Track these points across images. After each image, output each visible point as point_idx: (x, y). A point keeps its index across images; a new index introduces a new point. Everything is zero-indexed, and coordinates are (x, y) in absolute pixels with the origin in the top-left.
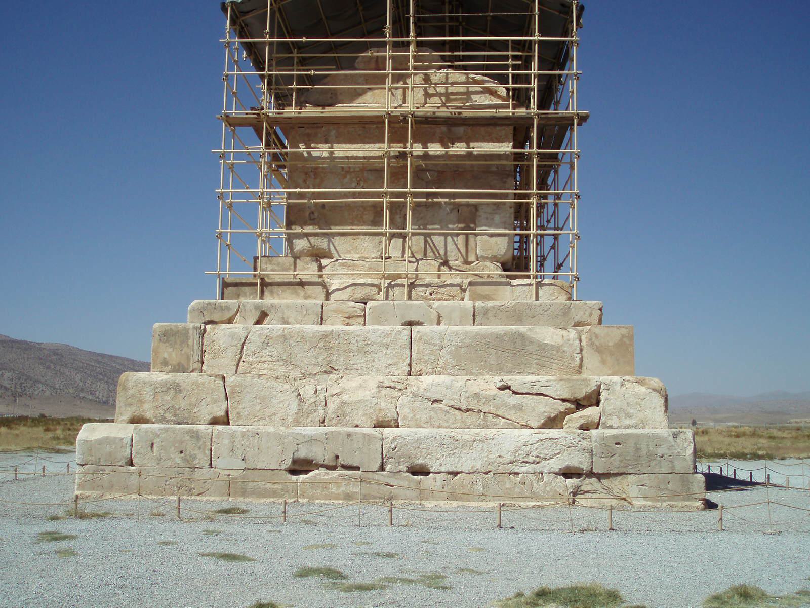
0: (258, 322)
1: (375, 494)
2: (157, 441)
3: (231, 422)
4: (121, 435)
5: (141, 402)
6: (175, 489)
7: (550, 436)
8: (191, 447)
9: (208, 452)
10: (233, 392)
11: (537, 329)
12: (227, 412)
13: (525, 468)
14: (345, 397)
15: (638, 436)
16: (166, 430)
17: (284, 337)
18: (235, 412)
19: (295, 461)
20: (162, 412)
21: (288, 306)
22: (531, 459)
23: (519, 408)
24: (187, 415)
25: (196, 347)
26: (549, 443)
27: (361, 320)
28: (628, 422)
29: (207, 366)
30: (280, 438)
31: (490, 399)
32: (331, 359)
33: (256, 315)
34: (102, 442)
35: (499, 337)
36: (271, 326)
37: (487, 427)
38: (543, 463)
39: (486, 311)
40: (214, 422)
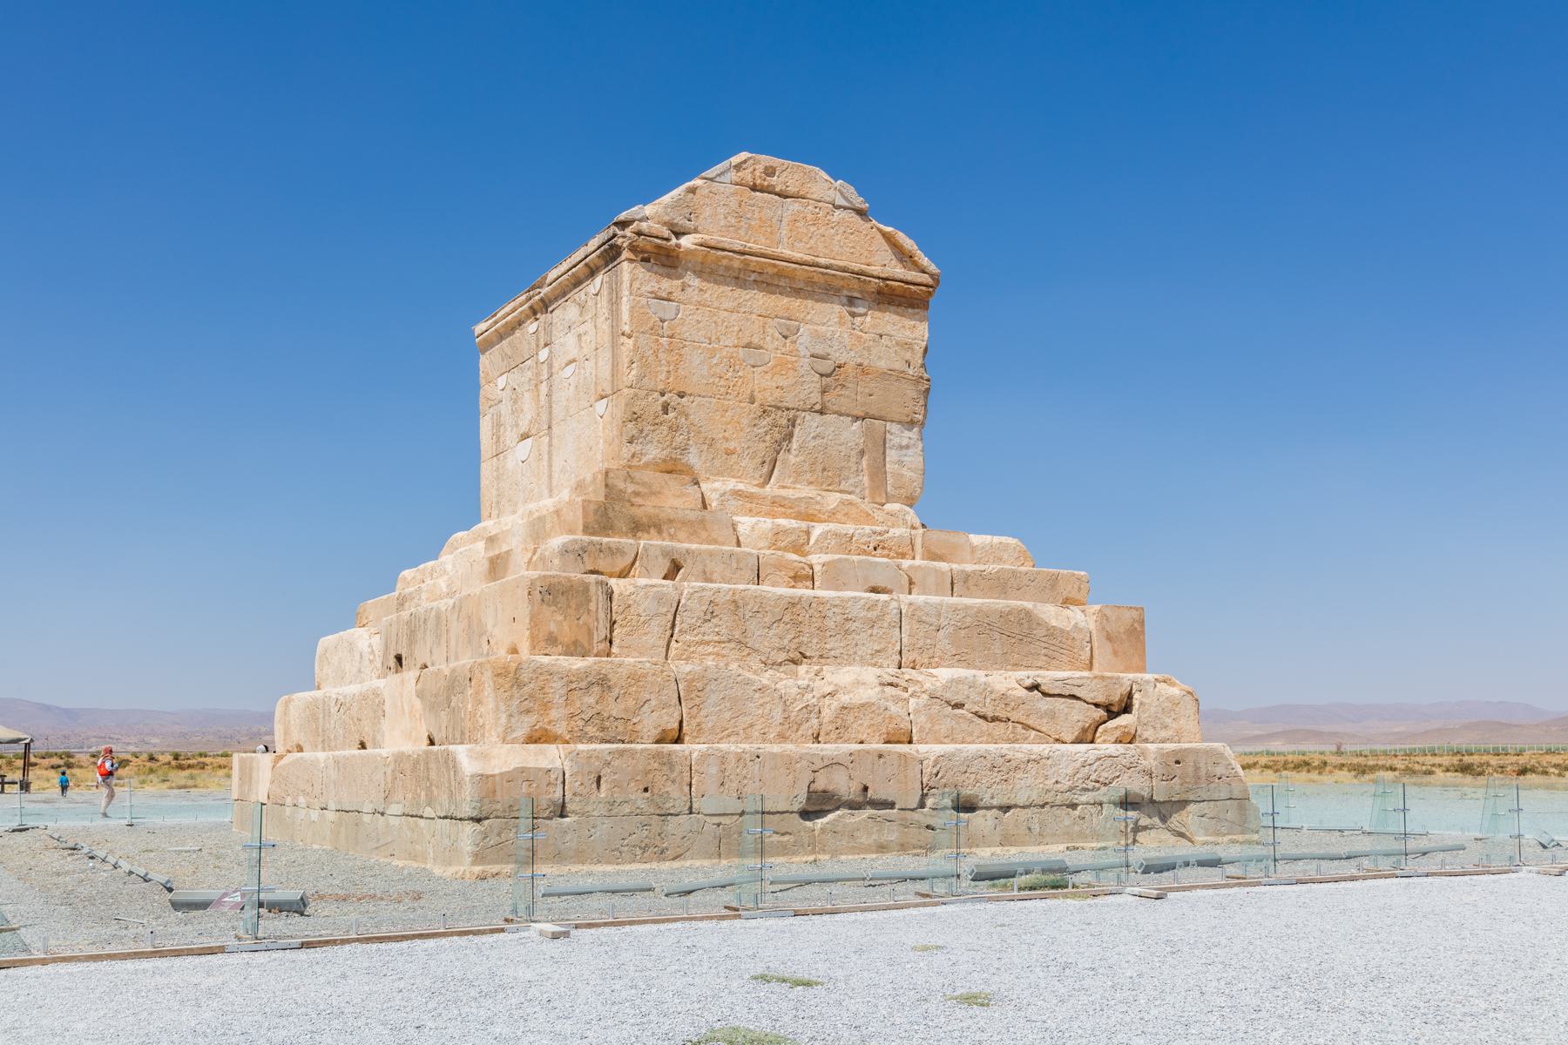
1: (914, 841)
3: (687, 738)
4: (544, 764)
5: (546, 706)
6: (639, 852)
9: (687, 789)
10: (689, 690)
12: (681, 722)
14: (845, 699)
16: (621, 753)
18: (694, 723)
20: (581, 723)
21: (711, 554)
22: (1091, 785)
23: (1052, 715)
24: (621, 729)
25: (602, 615)
26: (1108, 762)
27: (809, 583)
28: (1163, 734)
29: (621, 647)
30: (789, 762)
33: (666, 565)
35: (1002, 615)
36: (687, 585)
39: (967, 577)
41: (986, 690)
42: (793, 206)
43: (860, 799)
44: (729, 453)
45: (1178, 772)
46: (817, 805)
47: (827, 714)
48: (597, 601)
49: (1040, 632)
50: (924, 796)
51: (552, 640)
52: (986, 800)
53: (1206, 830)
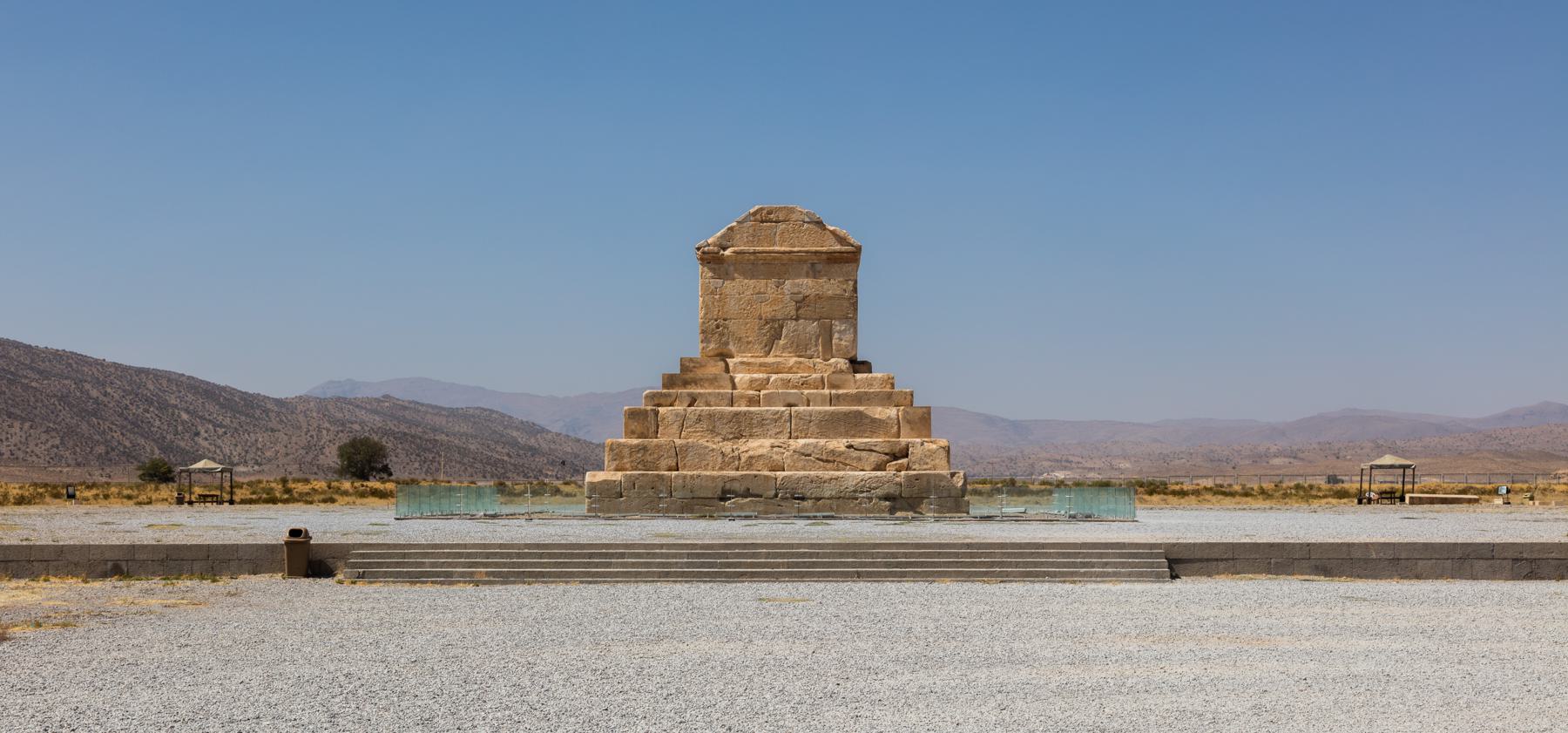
17: (711, 416)
23: (860, 459)
30: (713, 478)
31: (841, 454)
35: (846, 414)
36: (700, 408)
39: (838, 396)
40: (670, 469)
41: (823, 449)
42: (782, 226)
48: (651, 417)
51: (633, 432)
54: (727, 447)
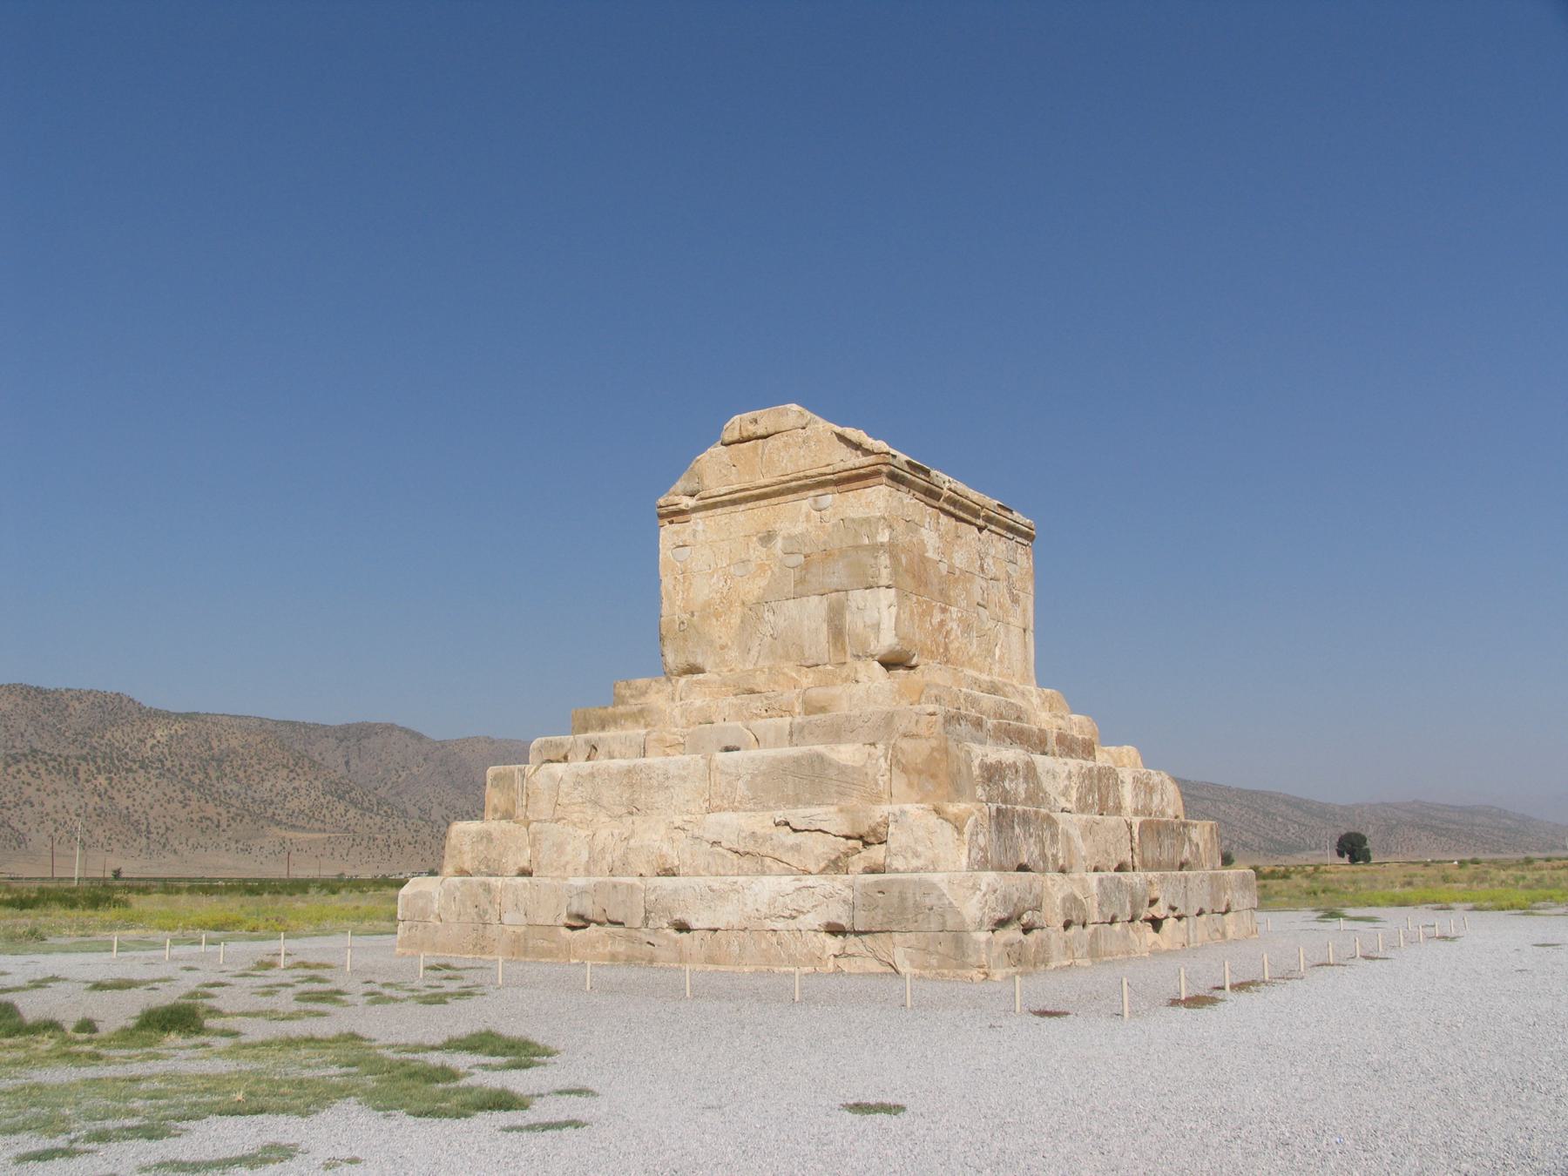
0: (589, 758)
2: (458, 894)
7: (809, 883)
8: (483, 899)
11: (842, 748)
13: (779, 925)
15: (902, 882)
17: (592, 775)
19: (570, 916)
21: (614, 738)
22: (787, 913)
23: (796, 848)
26: (805, 892)
28: (915, 863)
32: (636, 793)
34: (415, 896)
35: (797, 761)
36: (601, 762)
37: (764, 873)
38: (802, 917)
39: (802, 728)
43: (603, 919)
44: (722, 648)
45: (881, 903)
46: (580, 922)
47: (618, 853)
49: (832, 772)
50: (646, 919)
52: (694, 924)
53: (912, 961)
54: (607, 832)
